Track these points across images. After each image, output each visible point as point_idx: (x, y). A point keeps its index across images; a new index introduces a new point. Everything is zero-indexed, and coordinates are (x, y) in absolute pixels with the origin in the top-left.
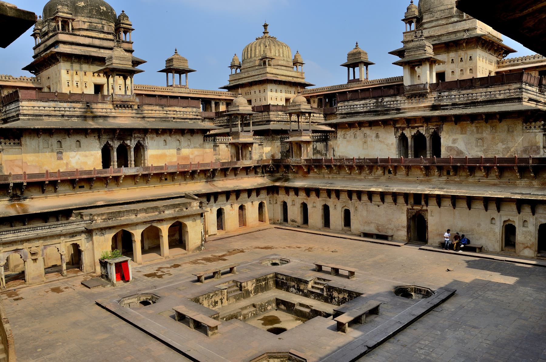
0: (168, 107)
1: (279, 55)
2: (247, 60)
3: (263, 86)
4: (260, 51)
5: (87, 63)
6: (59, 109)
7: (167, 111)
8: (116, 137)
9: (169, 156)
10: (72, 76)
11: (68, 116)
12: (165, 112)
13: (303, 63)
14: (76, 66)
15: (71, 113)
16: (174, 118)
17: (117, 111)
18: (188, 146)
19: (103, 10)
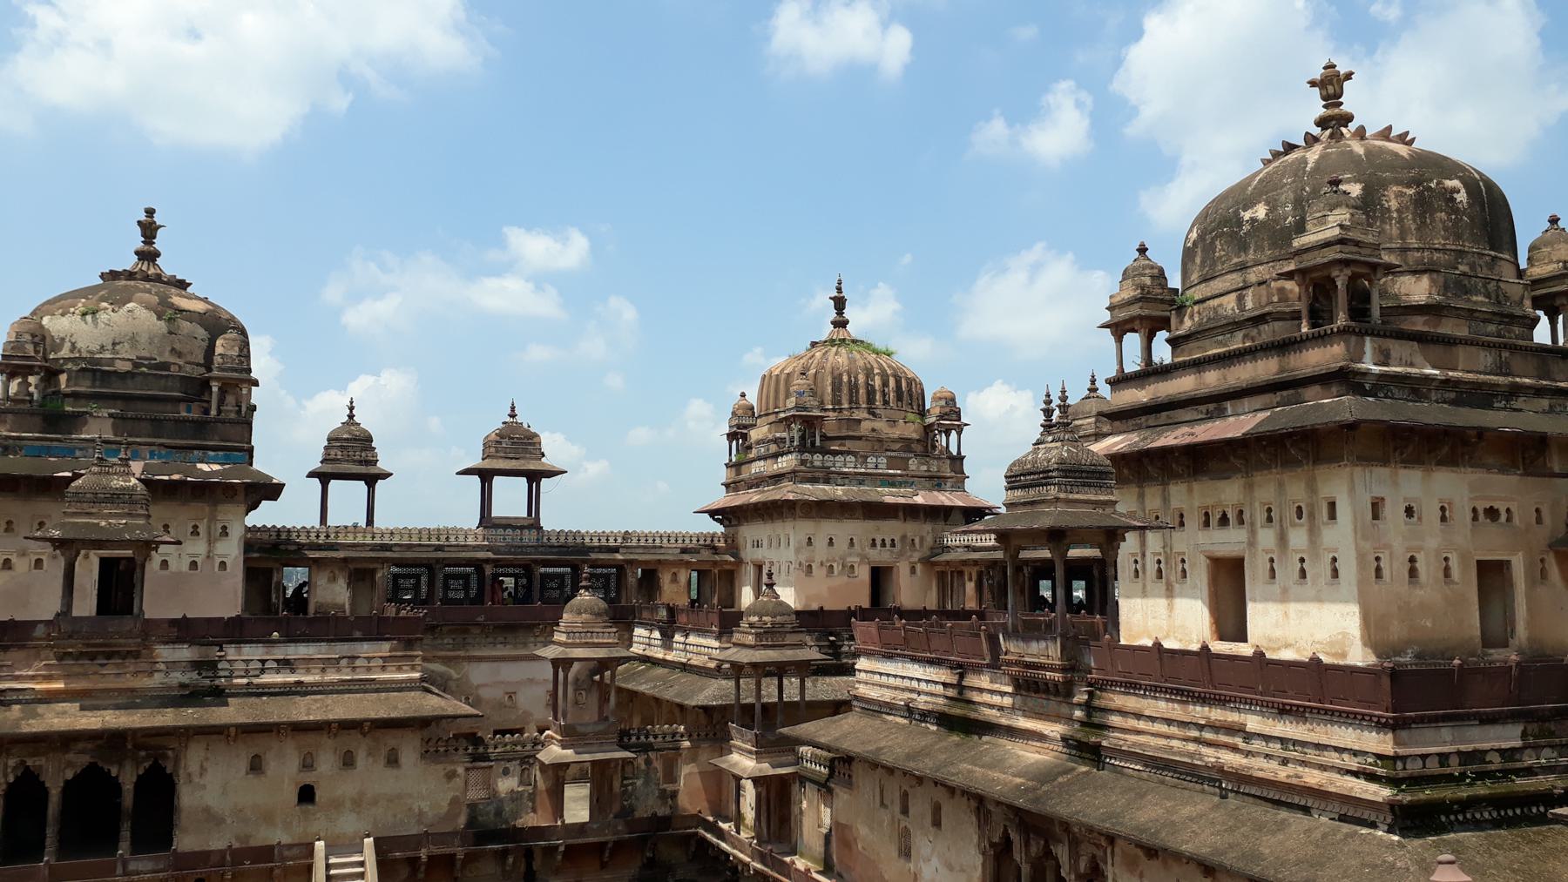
0: (1203, 700)
12: (1195, 733)
19: (1253, 220)
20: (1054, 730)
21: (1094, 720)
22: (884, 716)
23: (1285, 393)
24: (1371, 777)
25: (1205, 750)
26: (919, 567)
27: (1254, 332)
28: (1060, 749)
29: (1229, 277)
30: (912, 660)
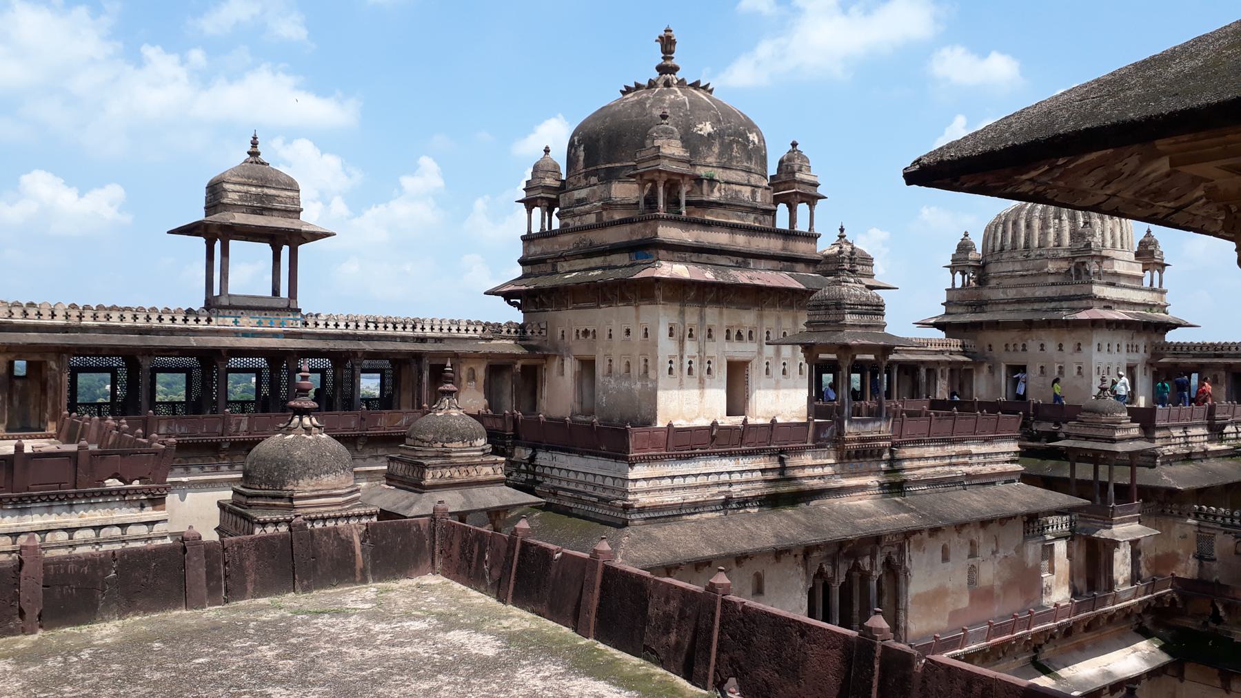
1: (1114, 246)
2: (1015, 254)
3: (1073, 335)
4: (1059, 235)
5: (718, 302)
7: (950, 457)
8: (845, 551)
9: (953, 593)
10: (681, 342)
12: (948, 461)
13: (1165, 262)
14: (692, 316)
18: (993, 557)
20: (871, 480)
21: (894, 465)
22: (684, 517)
23: (785, 263)
24: (1012, 462)
25: (953, 468)
27: (761, 218)
28: (878, 492)
29: (740, 173)
30: (720, 456)
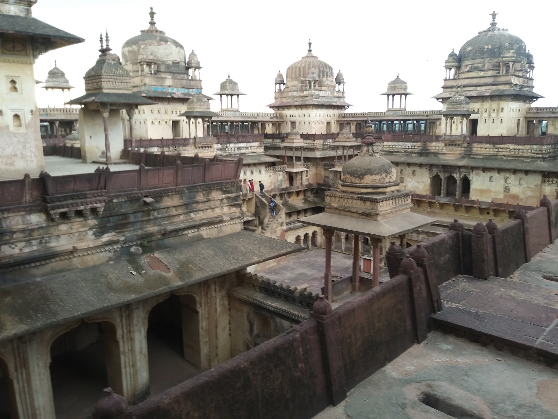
6: (404, 147)
9: (494, 192)
11: (410, 152)
12: (497, 150)
15: (412, 150)
16: (505, 156)
17: (448, 148)
26: (335, 122)
